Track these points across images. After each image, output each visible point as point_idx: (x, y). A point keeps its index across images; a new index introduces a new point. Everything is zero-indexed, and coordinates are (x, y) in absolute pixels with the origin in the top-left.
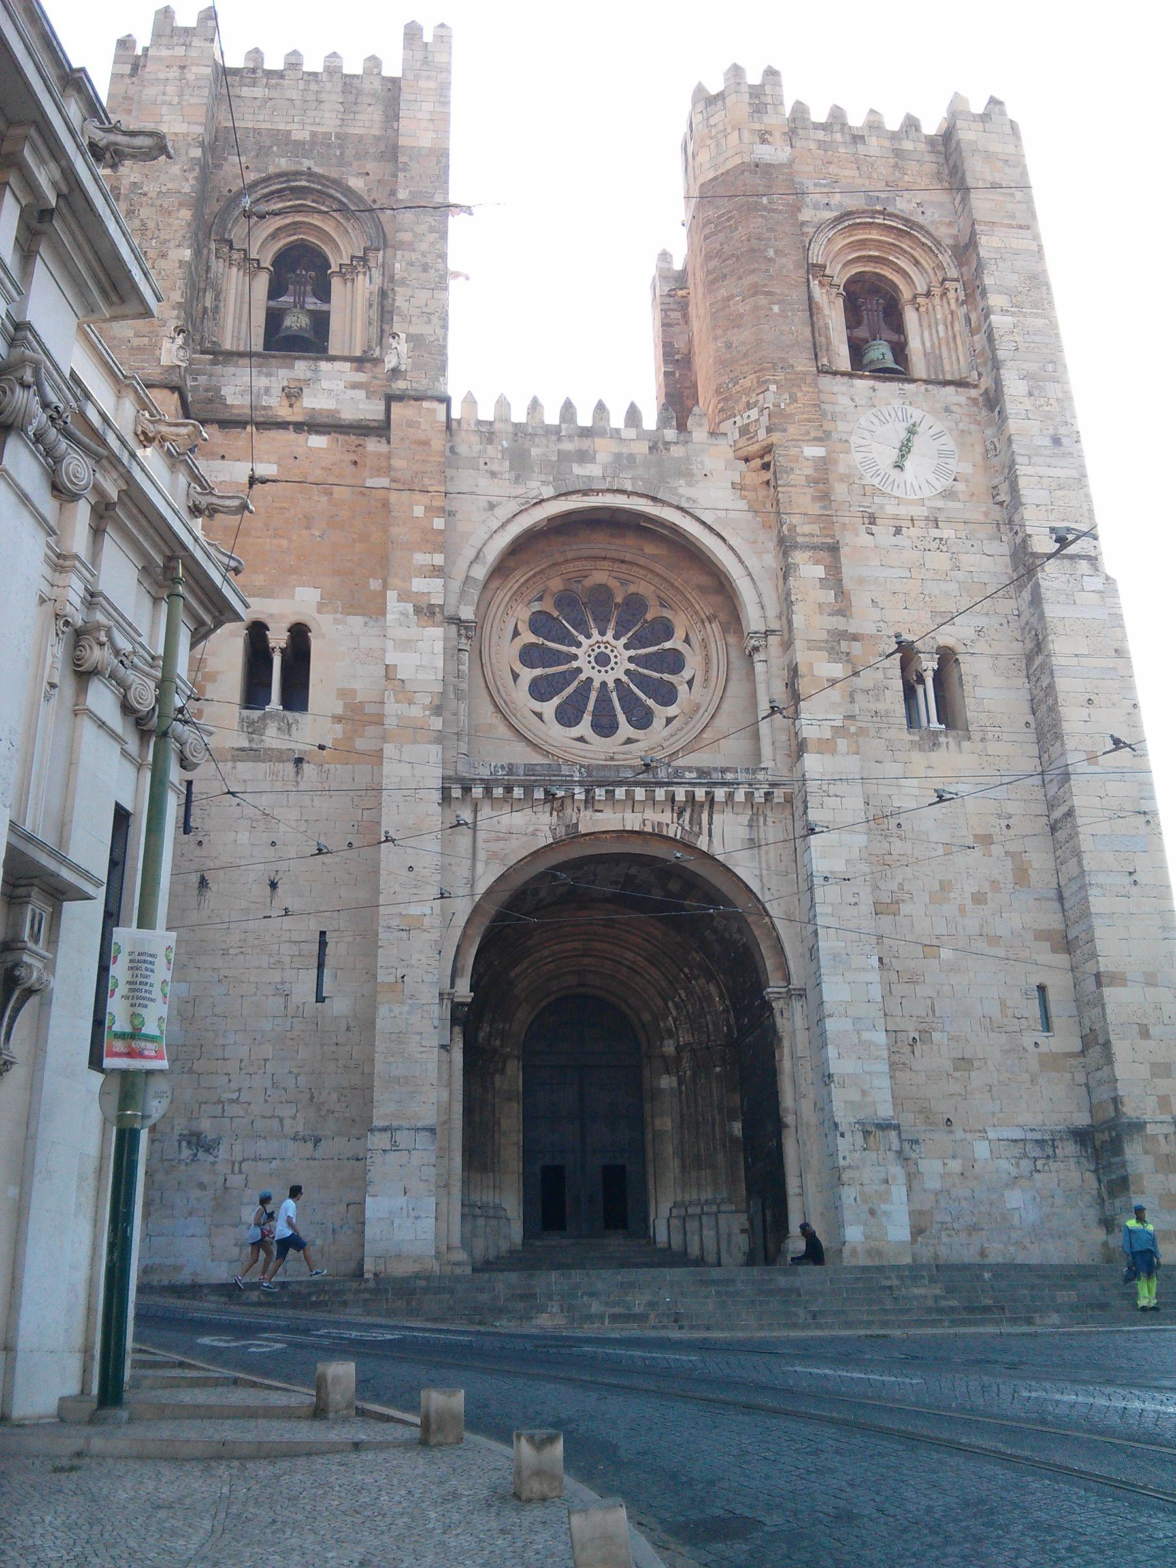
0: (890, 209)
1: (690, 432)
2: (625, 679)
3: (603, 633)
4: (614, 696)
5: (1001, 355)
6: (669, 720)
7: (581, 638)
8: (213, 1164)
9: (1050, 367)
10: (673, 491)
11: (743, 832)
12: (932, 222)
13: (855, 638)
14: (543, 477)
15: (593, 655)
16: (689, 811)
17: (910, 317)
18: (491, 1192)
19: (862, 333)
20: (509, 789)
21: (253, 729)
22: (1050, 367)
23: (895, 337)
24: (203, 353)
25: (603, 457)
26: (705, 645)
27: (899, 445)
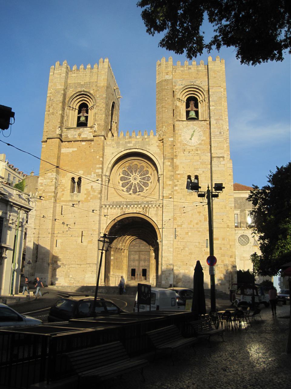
0: (195, 84)
1: (150, 136)
2: (139, 182)
3: (135, 174)
4: (137, 186)
5: (211, 115)
6: (147, 190)
7: (131, 175)
8: (65, 268)
9: (221, 117)
10: (146, 148)
11: (155, 212)
12: (203, 85)
13: (179, 174)
14: (122, 147)
15: (133, 178)
16: (145, 208)
17: (199, 104)
18: (121, 273)
19: (189, 109)
20: (113, 206)
21: (72, 196)
22: (221, 117)
23: (196, 109)
24: (65, 128)
25: (133, 142)
26: (154, 175)
27: (191, 135)
